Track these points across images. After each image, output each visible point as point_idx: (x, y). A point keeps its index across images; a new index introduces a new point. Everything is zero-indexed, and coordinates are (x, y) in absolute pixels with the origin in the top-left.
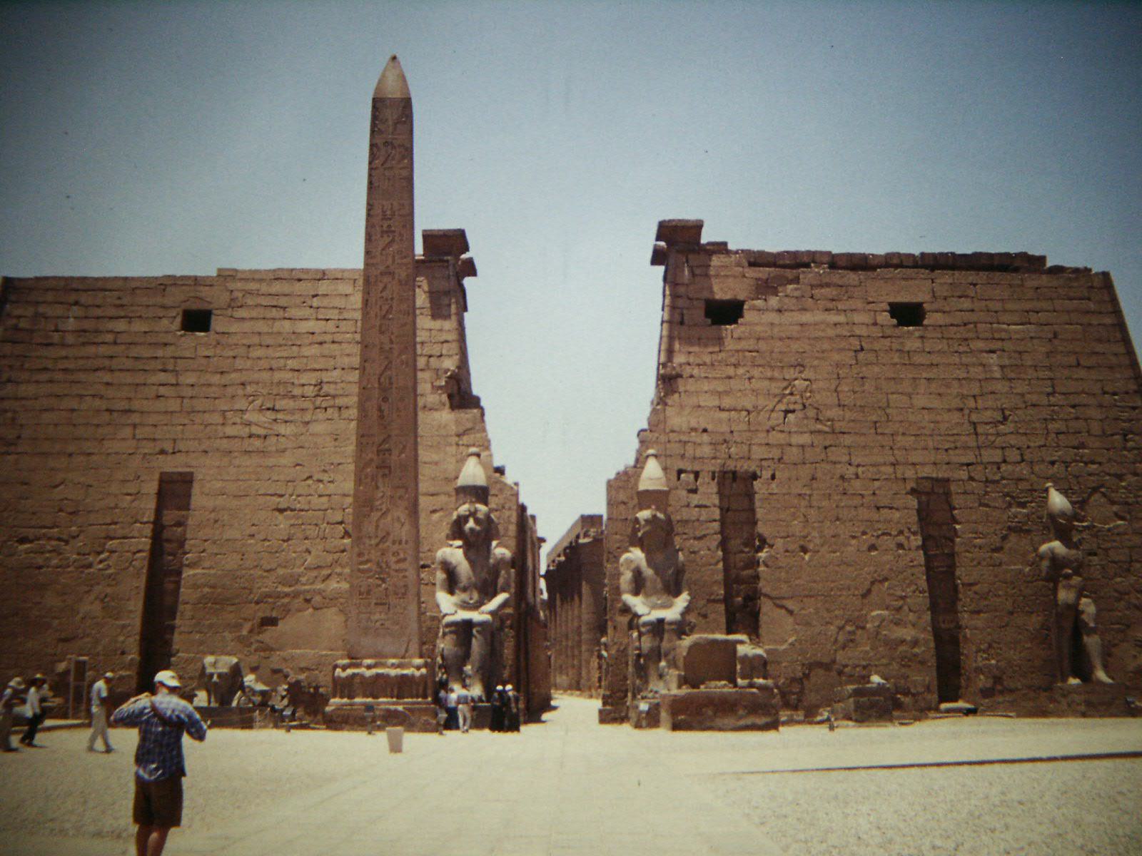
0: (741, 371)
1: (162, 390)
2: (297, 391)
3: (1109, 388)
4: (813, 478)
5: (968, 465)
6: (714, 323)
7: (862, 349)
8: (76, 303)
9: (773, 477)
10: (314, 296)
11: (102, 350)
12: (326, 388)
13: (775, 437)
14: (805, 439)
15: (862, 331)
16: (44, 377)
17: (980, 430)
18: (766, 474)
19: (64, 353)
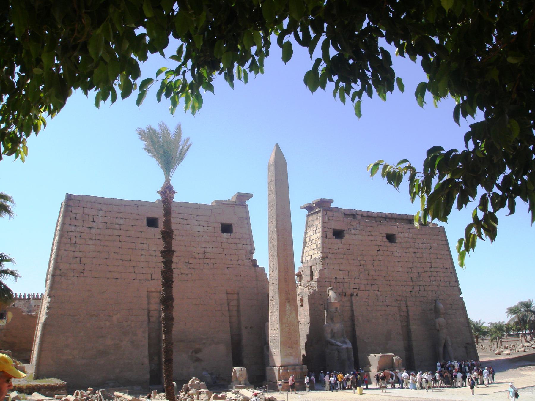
0: (345, 256)
1: (143, 253)
2: (197, 256)
3: (445, 267)
4: (369, 296)
5: (411, 291)
6: (336, 238)
7: (379, 250)
8: (101, 209)
9: (357, 295)
10: (198, 215)
11: (116, 232)
12: (207, 255)
13: (357, 281)
14: (365, 282)
15: (379, 243)
16: (90, 242)
17: (414, 279)
18: (355, 294)
19: (99, 231)
